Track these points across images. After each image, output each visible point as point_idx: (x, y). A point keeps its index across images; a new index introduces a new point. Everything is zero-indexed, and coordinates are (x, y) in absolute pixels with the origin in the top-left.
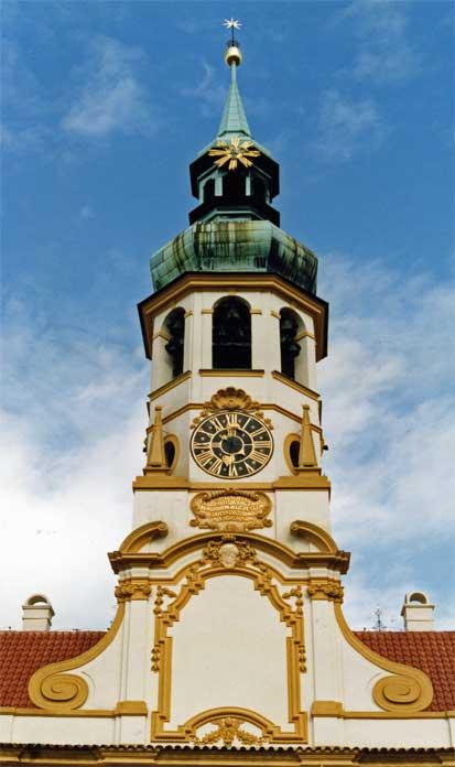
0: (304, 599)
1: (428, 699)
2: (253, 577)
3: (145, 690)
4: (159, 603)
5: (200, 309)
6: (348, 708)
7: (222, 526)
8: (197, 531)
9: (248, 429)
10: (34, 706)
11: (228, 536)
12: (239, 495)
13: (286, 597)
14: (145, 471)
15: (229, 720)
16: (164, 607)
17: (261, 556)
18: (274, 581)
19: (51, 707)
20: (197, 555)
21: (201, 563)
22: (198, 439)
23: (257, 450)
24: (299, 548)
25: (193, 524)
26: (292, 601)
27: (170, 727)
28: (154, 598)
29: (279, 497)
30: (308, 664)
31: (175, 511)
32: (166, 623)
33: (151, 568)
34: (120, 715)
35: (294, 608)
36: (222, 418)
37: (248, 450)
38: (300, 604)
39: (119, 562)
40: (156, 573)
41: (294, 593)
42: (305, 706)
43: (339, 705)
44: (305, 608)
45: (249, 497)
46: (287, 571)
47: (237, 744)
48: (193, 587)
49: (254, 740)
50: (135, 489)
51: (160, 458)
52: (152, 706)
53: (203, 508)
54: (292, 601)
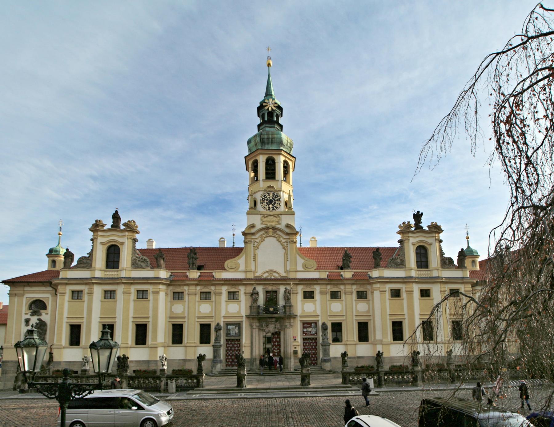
5: (262, 161)
7: (269, 224)
17: (278, 232)
18: (281, 239)
21: (264, 234)
24: (287, 230)
25: (262, 224)
26: (285, 244)
27: (257, 275)
29: (283, 217)
31: (257, 220)
36: (268, 194)
37: (275, 203)
39: (244, 234)
40: (253, 237)
41: (286, 242)
42: (288, 269)
44: (288, 246)
46: (284, 236)
47: (273, 278)
51: (253, 205)
52: (253, 269)
53: (264, 219)
54: (285, 244)
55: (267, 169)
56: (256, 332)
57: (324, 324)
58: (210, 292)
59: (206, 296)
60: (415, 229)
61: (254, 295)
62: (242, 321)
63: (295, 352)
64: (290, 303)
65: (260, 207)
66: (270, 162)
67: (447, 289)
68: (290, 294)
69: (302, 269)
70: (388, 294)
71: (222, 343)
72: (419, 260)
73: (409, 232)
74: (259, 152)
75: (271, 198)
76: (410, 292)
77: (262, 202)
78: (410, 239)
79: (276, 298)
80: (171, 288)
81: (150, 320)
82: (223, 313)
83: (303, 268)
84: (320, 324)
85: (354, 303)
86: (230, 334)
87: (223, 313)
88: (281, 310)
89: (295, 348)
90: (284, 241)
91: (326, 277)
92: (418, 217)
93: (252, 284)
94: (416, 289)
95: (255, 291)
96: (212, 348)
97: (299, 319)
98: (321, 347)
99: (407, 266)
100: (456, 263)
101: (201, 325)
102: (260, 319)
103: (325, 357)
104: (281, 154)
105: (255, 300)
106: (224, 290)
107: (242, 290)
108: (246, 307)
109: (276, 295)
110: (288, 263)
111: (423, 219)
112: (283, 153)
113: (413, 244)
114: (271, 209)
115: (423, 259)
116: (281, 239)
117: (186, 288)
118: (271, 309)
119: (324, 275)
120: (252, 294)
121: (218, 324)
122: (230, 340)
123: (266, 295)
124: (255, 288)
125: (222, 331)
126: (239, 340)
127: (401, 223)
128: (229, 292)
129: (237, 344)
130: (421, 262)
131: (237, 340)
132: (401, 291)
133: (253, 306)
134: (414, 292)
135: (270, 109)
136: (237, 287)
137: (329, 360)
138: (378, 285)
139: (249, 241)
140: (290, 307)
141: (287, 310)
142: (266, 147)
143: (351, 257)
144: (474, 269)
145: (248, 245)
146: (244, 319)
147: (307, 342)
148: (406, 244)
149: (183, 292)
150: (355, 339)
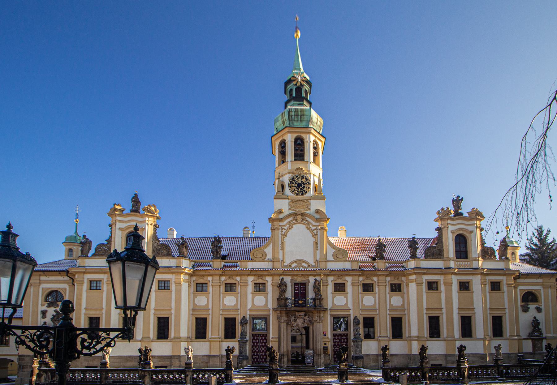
4: (282, 232)
7: (297, 210)
8: (291, 212)
13: (314, 230)
17: (308, 219)
19: (257, 260)
20: (291, 219)
24: (317, 216)
27: (286, 264)
28: (280, 230)
29: (313, 202)
37: (304, 187)
40: (281, 224)
42: (318, 258)
44: (318, 233)
47: (301, 268)
52: (281, 258)
54: (315, 231)
55: (295, 150)
56: (284, 326)
57: (355, 318)
58: (236, 284)
59: (230, 288)
60: (454, 216)
62: (269, 315)
63: (325, 349)
65: (287, 191)
66: (299, 142)
68: (320, 286)
70: (424, 287)
71: (248, 338)
72: (458, 248)
73: (448, 219)
74: (287, 130)
75: (300, 182)
76: (448, 285)
78: (450, 226)
79: (305, 290)
80: (194, 278)
81: (173, 311)
82: (249, 306)
83: (334, 258)
84: (352, 318)
85: (388, 296)
86: (256, 328)
87: (249, 306)
88: (310, 303)
89: (325, 344)
90: (313, 228)
92: (457, 202)
93: (281, 275)
94: (455, 280)
96: (237, 343)
97: (329, 312)
98: (352, 343)
99: (445, 256)
101: (225, 318)
102: (289, 313)
104: (310, 133)
105: (283, 291)
106: (251, 280)
108: (273, 300)
109: (305, 288)
110: (318, 252)
111: (463, 205)
112: (313, 131)
113: (453, 232)
114: (299, 193)
115: (462, 251)
116: (311, 226)
117: (210, 278)
118: (301, 302)
120: (280, 286)
122: (256, 335)
123: (295, 288)
125: (248, 325)
126: (266, 336)
128: (255, 284)
129: (263, 340)
130: (460, 251)
131: (263, 335)
134: (453, 284)
135: (299, 84)
136: (264, 278)
137: (361, 358)
138: (414, 277)
139: (277, 228)
140: (320, 299)
142: (296, 124)
143: (385, 247)
145: (276, 232)
146: (271, 312)
147: (338, 339)
150: (389, 335)
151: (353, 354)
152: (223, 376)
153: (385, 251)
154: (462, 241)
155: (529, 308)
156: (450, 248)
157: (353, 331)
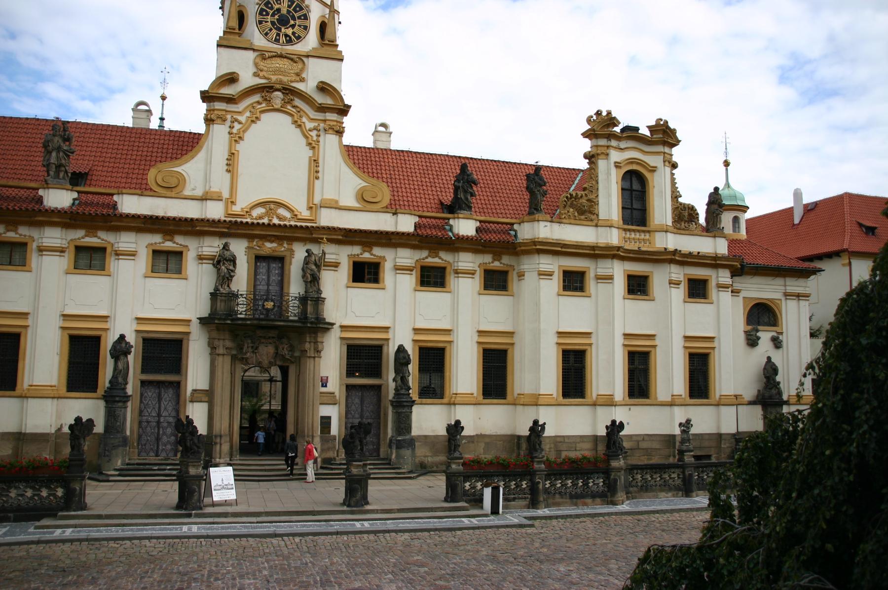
0: (322, 133)
1: (386, 201)
2: (291, 115)
3: (220, 183)
4: (231, 127)
6: (343, 203)
7: (274, 78)
9: (294, 10)
10: (151, 189)
11: (278, 86)
12: (286, 57)
14: (224, 32)
15: (272, 206)
16: (235, 131)
17: (298, 102)
18: (304, 119)
21: (259, 103)
22: (261, 14)
23: (299, 26)
24: (320, 99)
25: (256, 75)
27: (237, 209)
28: (228, 123)
29: (312, 63)
30: (320, 175)
32: (236, 141)
33: (227, 103)
34: (206, 199)
35: (315, 138)
38: (318, 136)
39: (206, 97)
41: (315, 129)
43: (337, 202)
44: (321, 139)
45: (292, 60)
46: (312, 114)
47: (276, 221)
48: (254, 119)
49: (284, 219)
50: (218, 46)
51: (235, 23)
52: (226, 195)
53: (262, 64)
56: (224, 364)
57: (401, 350)
59: (90, 259)
61: (223, 264)
62: (188, 334)
64: (319, 291)
67: (682, 279)
68: (318, 267)
69: (356, 205)
77: (259, 18)
83: (358, 201)
91: (411, 229)
94: (619, 271)
95: (227, 254)
99: (601, 217)
100: (702, 220)
103: (400, 434)
105: (225, 278)
107: (194, 249)
113: (617, 165)
115: (636, 207)
119: (406, 224)
120: (219, 262)
121: (122, 337)
124: (226, 247)
125: (131, 358)
127: (592, 112)
130: (632, 209)
132: (587, 275)
133: (221, 296)
139: (219, 117)
141: (310, 309)
144: (736, 236)
148: (601, 164)
149: (25, 245)
151: (390, 433)
152: (60, 492)
153: (472, 195)
154: (636, 187)
155: (759, 338)
156: (610, 201)
157: (394, 380)
